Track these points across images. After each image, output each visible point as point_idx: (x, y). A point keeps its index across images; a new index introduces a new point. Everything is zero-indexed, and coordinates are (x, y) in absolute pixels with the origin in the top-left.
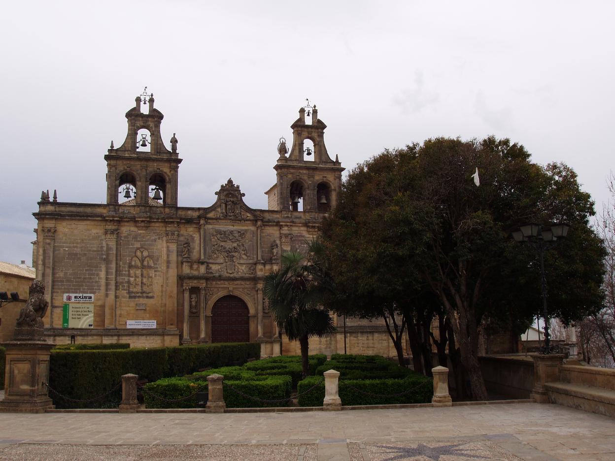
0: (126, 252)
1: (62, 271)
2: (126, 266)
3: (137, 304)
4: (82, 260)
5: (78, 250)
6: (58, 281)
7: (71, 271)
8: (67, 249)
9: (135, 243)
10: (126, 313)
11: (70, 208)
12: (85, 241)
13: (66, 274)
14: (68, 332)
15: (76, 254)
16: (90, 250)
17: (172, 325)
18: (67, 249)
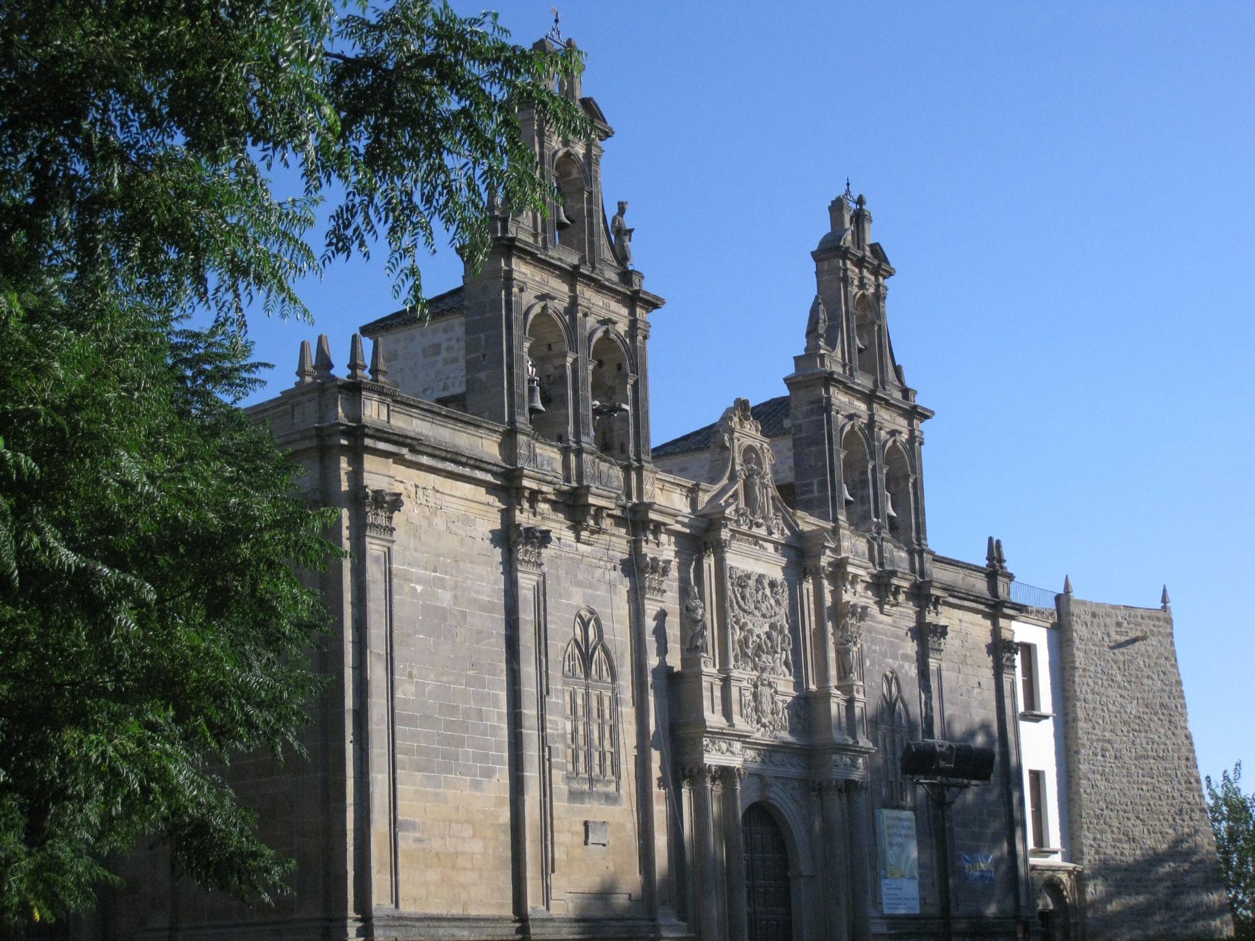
0: (556, 623)
1: (410, 676)
2: (560, 675)
3: (586, 824)
4: (458, 640)
5: (445, 598)
6: (411, 720)
7: (431, 684)
8: (419, 588)
9: (574, 589)
10: (564, 857)
11: (418, 421)
12: (461, 564)
13: (421, 687)
14: (441, 931)
15: (443, 614)
16: (474, 601)
17: (664, 902)
18: (419, 588)
